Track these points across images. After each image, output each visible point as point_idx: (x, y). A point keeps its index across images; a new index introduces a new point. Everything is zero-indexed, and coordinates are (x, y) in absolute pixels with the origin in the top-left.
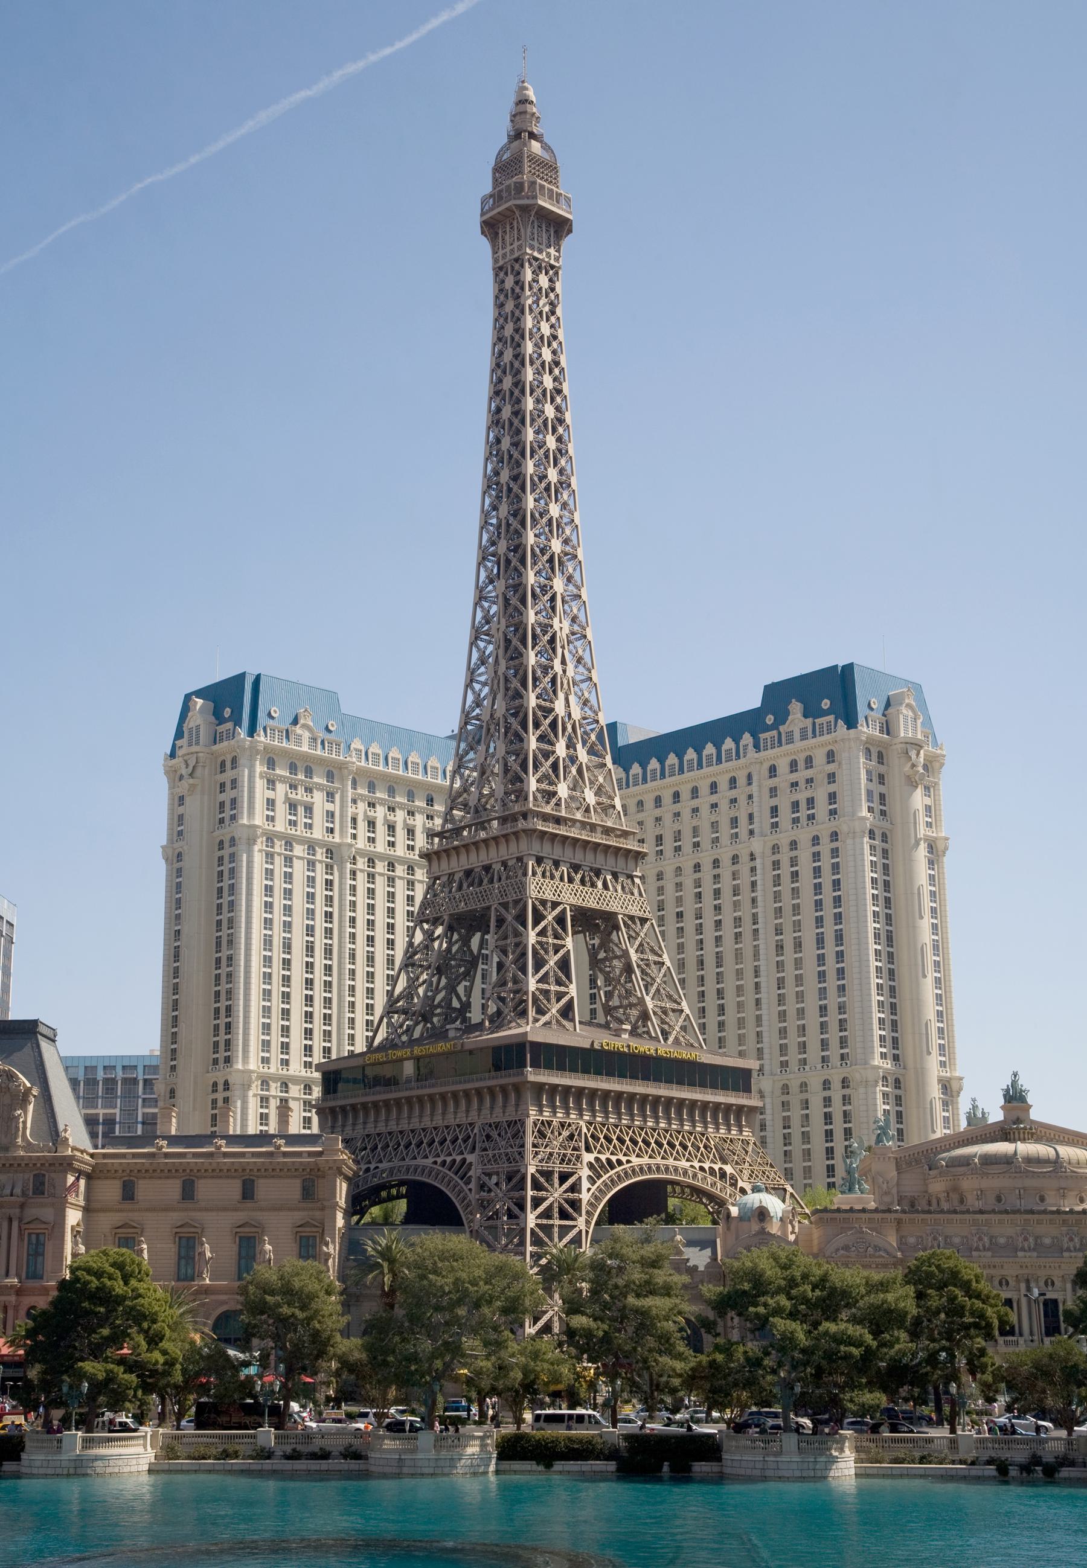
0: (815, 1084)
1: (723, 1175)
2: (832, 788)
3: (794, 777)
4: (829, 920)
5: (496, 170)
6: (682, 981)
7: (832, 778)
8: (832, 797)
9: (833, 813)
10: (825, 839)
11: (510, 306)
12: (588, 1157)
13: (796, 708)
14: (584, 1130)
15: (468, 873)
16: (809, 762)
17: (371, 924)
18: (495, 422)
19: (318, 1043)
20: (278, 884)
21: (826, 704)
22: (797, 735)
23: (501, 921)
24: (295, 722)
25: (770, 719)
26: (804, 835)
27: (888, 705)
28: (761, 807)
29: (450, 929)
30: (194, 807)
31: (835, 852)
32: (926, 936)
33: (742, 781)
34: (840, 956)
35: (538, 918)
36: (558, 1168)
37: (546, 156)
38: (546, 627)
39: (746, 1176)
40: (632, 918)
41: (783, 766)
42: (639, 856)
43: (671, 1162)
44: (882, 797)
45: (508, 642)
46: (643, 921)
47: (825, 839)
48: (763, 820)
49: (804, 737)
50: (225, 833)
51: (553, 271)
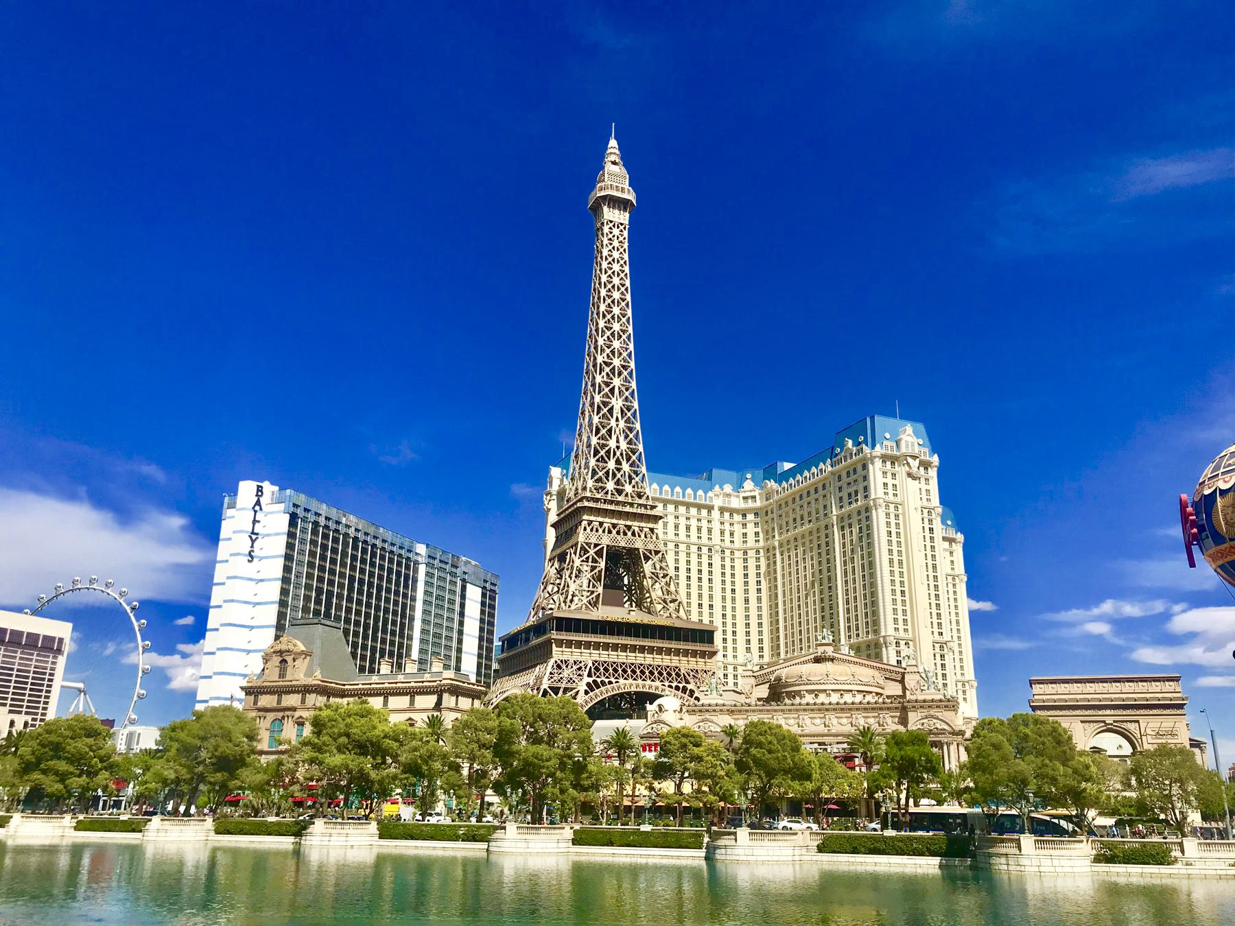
3: (849, 480)
7: (865, 478)
12: (590, 680)
14: (590, 664)
16: (855, 470)
38: (605, 404)
42: (656, 519)
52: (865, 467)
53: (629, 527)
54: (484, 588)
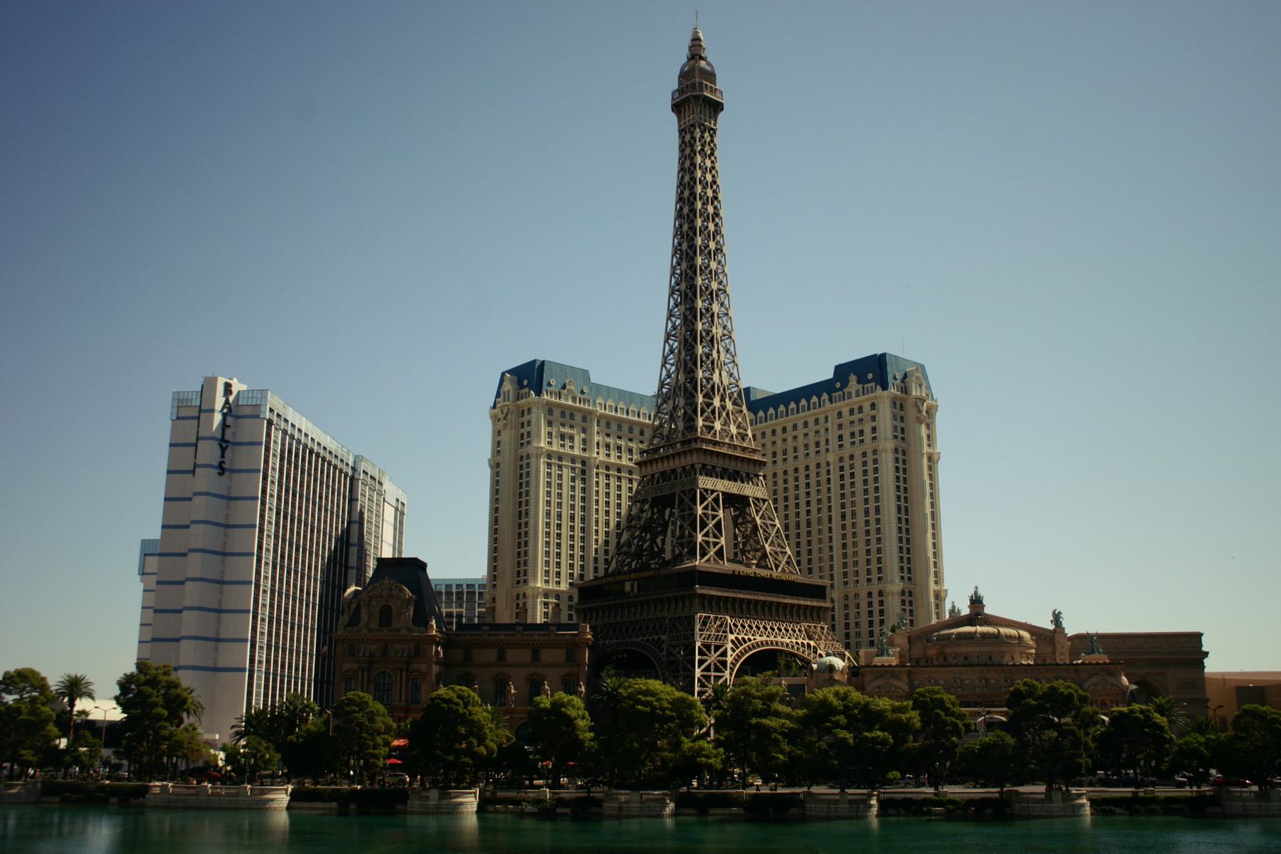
0: (863, 594)
1: (809, 645)
2: (874, 424)
3: (852, 418)
4: (872, 500)
5: (680, 76)
6: (787, 536)
7: (873, 419)
8: (874, 430)
9: (874, 438)
10: (870, 454)
11: (688, 151)
12: (731, 637)
13: (853, 378)
15: (663, 473)
16: (860, 409)
17: (607, 503)
18: (679, 215)
19: (577, 571)
20: (555, 481)
21: (870, 376)
22: (854, 394)
23: (681, 501)
24: (564, 387)
25: (838, 385)
26: (857, 452)
27: (905, 376)
28: (833, 436)
29: (652, 507)
30: (506, 436)
31: (875, 461)
32: (928, 510)
33: (822, 420)
34: (878, 521)
35: (703, 499)
36: (714, 643)
37: (708, 68)
38: (708, 332)
39: (822, 646)
40: (757, 499)
41: (845, 411)
42: (762, 464)
43: (779, 639)
44: (903, 429)
45: (686, 341)
46: (764, 501)
47: (870, 454)
48: (834, 443)
49: (858, 395)
50: (523, 451)
51: (713, 132)
52: (873, 406)
53: (737, 473)
54: (397, 509)
